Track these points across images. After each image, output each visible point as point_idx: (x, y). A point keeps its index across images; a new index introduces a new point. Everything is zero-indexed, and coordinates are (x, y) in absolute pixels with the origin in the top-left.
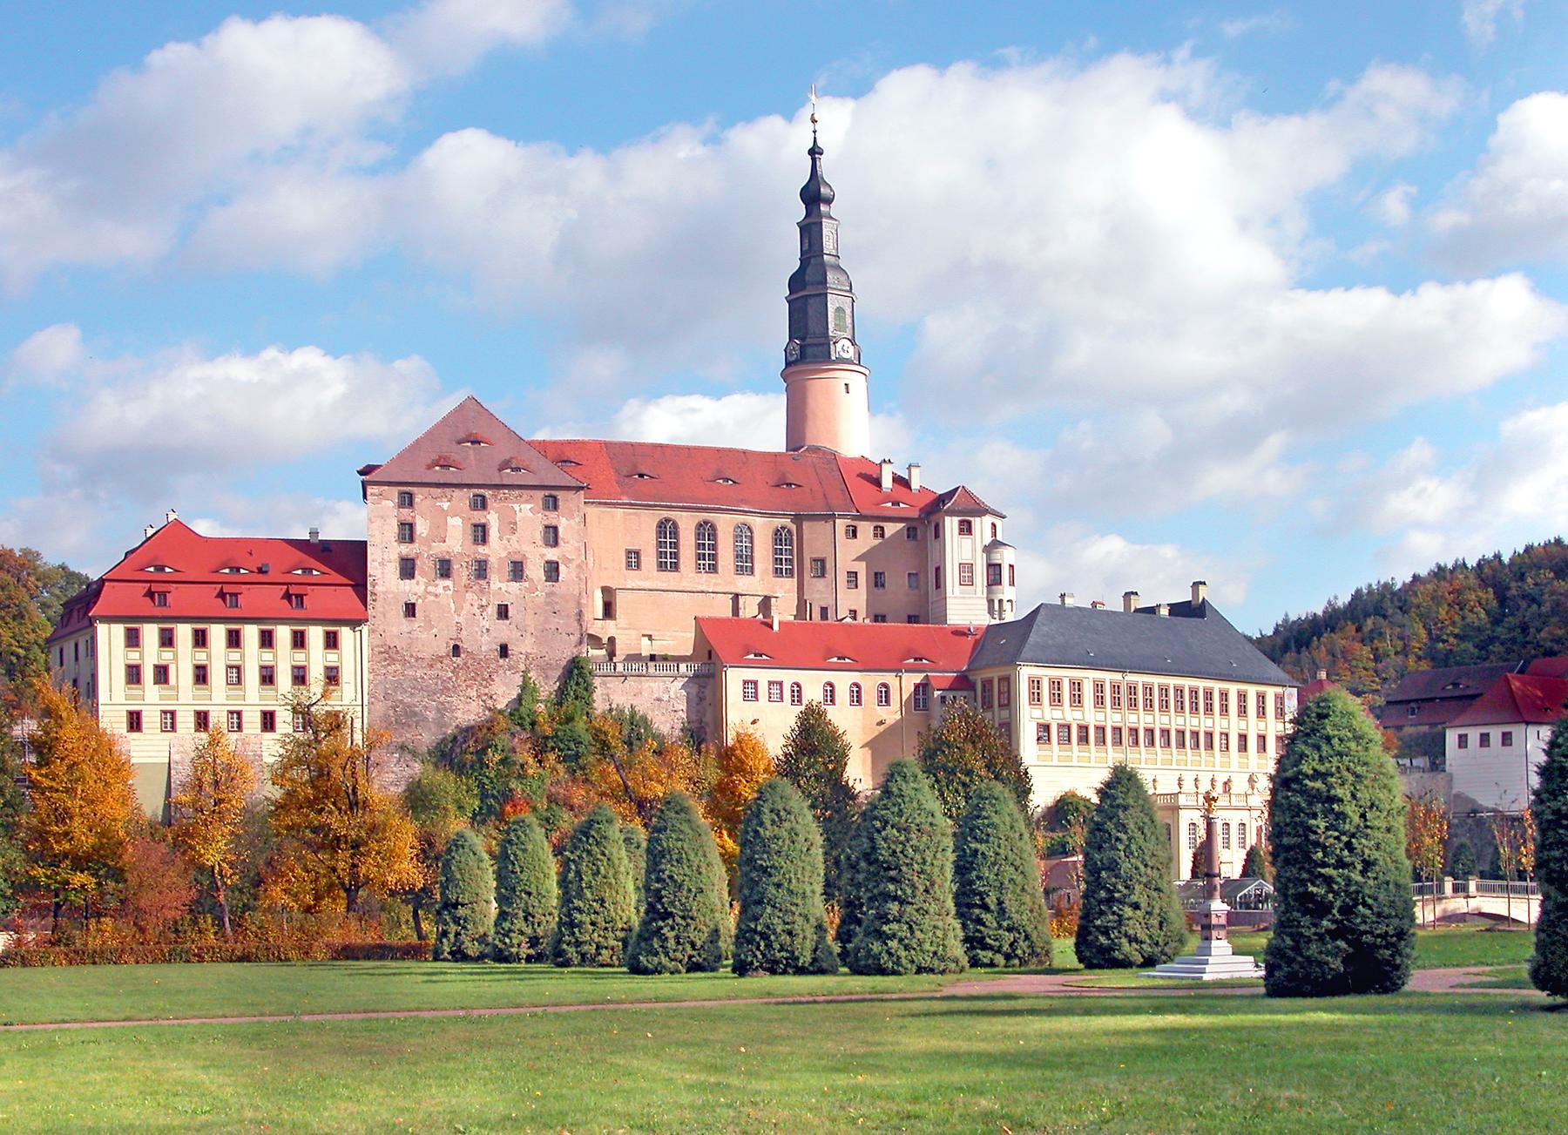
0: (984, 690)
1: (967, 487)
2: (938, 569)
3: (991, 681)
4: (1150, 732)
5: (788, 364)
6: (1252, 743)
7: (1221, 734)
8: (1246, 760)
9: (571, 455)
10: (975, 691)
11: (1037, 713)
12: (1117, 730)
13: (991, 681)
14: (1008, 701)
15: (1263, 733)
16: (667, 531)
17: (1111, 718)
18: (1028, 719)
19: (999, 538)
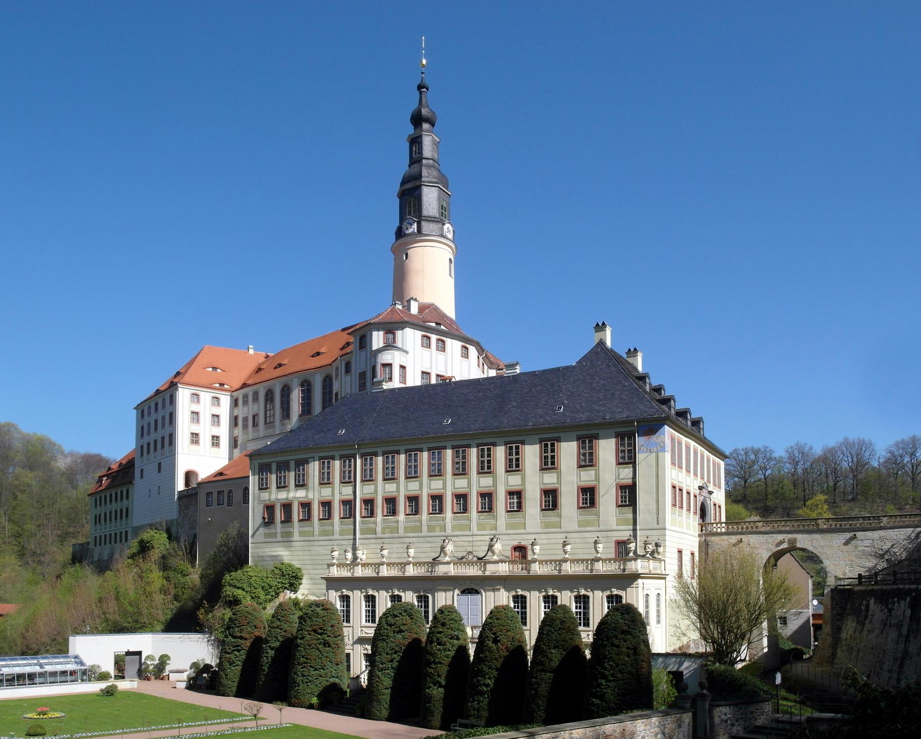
6: (569, 499)
7: (511, 493)
11: (265, 496)
16: (269, 396)
17: (338, 492)
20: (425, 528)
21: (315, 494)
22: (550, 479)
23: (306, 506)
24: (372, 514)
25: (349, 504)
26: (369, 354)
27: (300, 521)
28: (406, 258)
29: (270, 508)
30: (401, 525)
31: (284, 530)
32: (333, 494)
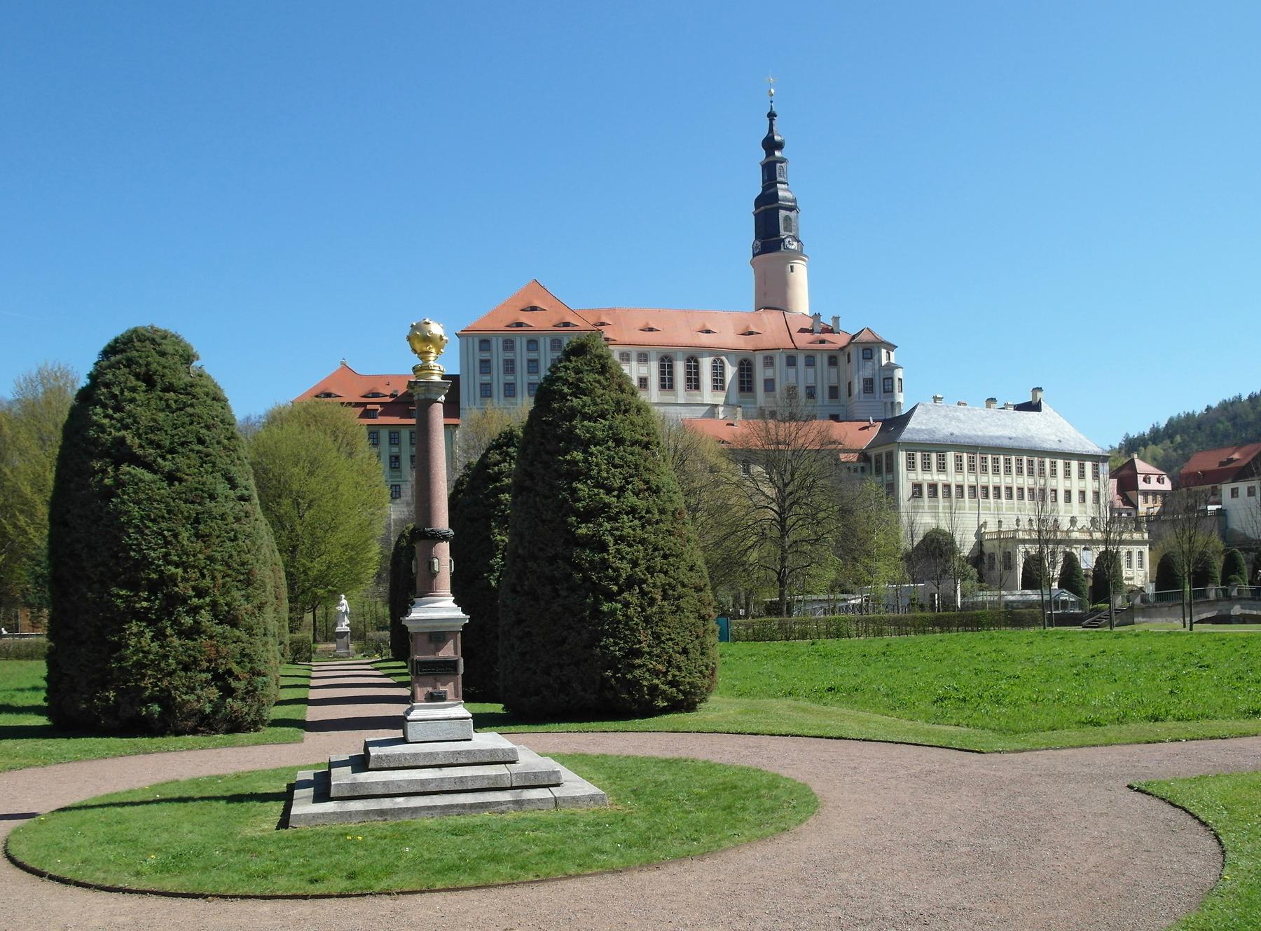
0: (876, 462)
1: (870, 328)
2: (850, 383)
3: (880, 455)
4: (1009, 489)
5: (754, 255)
6: (1075, 496)
8: (1070, 508)
9: (604, 319)
10: (871, 463)
12: (973, 488)
13: (880, 455)
14: (891, 467)
15: (1083, 489)
17: (967, 479)
18: (906, 480)
19: (892, 361)
20: (1016, 509)
21: (951, 477)
22: (1068, 483)
23: (947, 487)
24: (987, 496)
25: (973, 488)
26: (877, 367)
27: (943, 497)
28: (792, 271)
29: (917, 487)
30: (1004, 505)
31: (932, 504)
32: (964, 480)
